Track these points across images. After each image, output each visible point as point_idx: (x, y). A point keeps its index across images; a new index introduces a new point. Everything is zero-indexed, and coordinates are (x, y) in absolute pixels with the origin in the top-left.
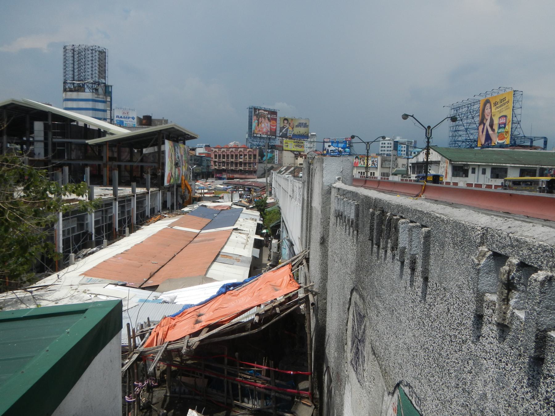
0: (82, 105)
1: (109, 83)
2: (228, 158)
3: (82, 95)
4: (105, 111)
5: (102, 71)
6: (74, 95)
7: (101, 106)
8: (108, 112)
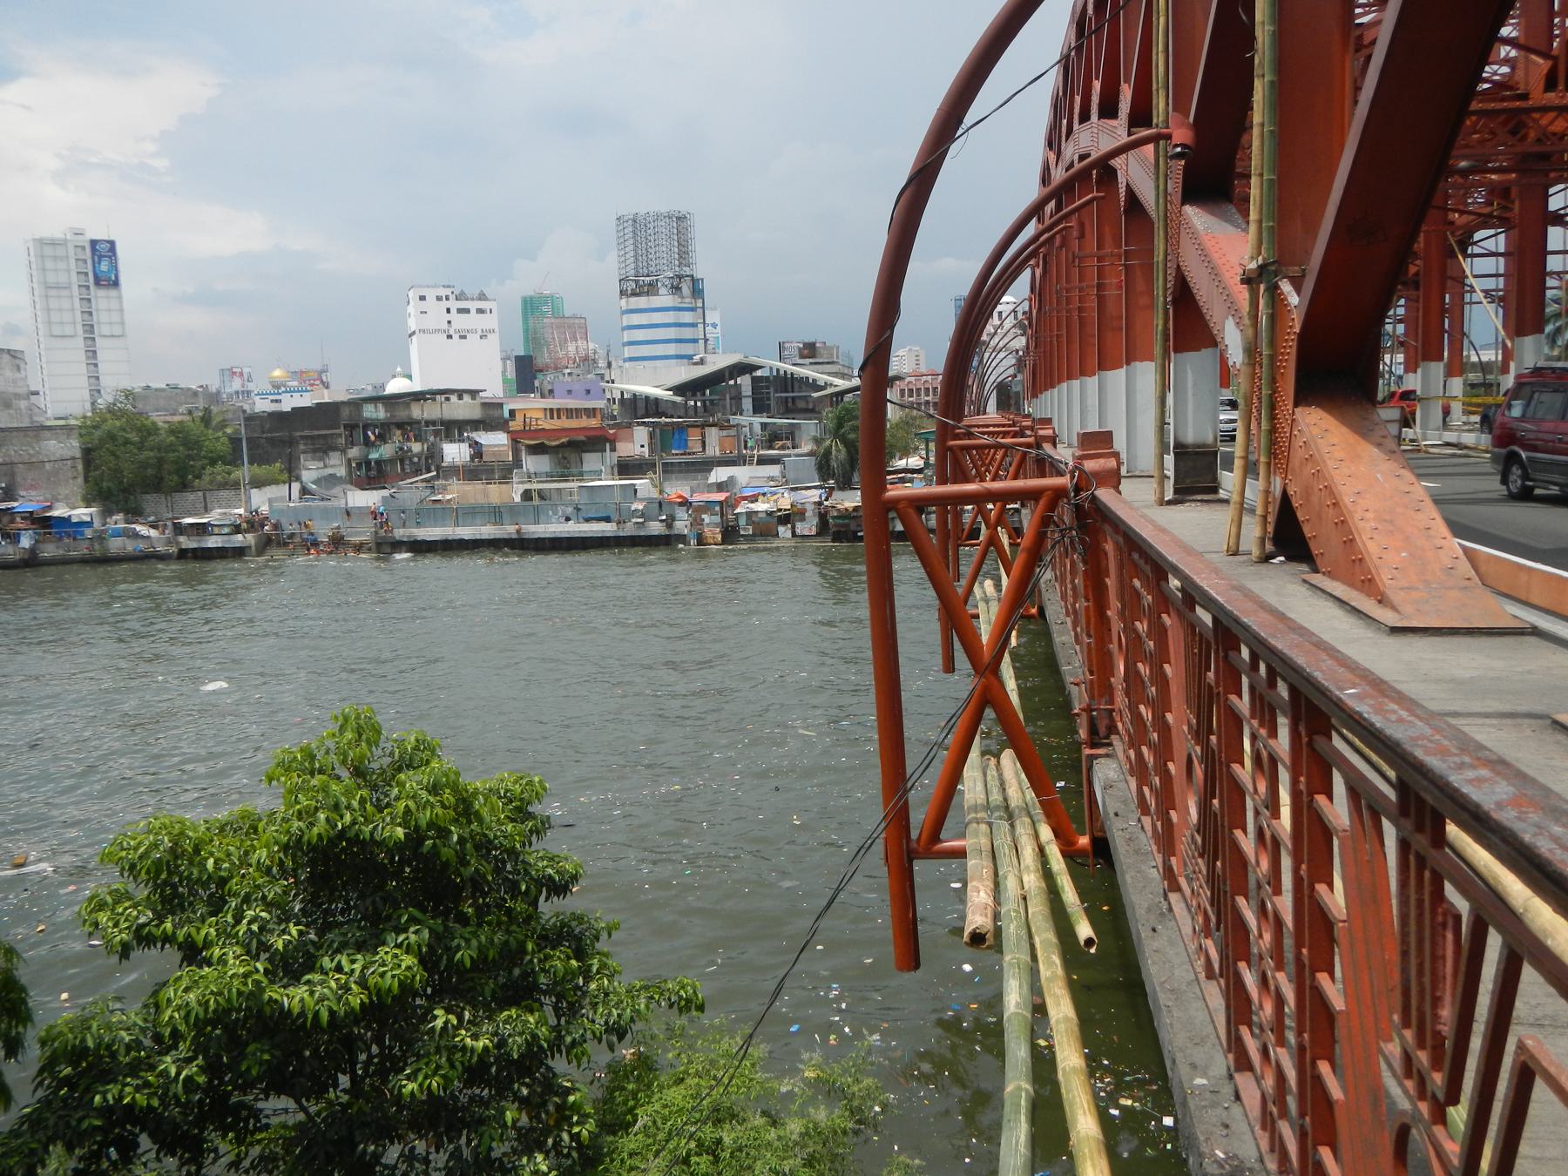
0: (657, 318)
1: (698, 275)
3: (656, 301)
4: (694, 325)
5: (684, 255)
6: (642, 302)
7: (687, 317)
8: (701, 326)
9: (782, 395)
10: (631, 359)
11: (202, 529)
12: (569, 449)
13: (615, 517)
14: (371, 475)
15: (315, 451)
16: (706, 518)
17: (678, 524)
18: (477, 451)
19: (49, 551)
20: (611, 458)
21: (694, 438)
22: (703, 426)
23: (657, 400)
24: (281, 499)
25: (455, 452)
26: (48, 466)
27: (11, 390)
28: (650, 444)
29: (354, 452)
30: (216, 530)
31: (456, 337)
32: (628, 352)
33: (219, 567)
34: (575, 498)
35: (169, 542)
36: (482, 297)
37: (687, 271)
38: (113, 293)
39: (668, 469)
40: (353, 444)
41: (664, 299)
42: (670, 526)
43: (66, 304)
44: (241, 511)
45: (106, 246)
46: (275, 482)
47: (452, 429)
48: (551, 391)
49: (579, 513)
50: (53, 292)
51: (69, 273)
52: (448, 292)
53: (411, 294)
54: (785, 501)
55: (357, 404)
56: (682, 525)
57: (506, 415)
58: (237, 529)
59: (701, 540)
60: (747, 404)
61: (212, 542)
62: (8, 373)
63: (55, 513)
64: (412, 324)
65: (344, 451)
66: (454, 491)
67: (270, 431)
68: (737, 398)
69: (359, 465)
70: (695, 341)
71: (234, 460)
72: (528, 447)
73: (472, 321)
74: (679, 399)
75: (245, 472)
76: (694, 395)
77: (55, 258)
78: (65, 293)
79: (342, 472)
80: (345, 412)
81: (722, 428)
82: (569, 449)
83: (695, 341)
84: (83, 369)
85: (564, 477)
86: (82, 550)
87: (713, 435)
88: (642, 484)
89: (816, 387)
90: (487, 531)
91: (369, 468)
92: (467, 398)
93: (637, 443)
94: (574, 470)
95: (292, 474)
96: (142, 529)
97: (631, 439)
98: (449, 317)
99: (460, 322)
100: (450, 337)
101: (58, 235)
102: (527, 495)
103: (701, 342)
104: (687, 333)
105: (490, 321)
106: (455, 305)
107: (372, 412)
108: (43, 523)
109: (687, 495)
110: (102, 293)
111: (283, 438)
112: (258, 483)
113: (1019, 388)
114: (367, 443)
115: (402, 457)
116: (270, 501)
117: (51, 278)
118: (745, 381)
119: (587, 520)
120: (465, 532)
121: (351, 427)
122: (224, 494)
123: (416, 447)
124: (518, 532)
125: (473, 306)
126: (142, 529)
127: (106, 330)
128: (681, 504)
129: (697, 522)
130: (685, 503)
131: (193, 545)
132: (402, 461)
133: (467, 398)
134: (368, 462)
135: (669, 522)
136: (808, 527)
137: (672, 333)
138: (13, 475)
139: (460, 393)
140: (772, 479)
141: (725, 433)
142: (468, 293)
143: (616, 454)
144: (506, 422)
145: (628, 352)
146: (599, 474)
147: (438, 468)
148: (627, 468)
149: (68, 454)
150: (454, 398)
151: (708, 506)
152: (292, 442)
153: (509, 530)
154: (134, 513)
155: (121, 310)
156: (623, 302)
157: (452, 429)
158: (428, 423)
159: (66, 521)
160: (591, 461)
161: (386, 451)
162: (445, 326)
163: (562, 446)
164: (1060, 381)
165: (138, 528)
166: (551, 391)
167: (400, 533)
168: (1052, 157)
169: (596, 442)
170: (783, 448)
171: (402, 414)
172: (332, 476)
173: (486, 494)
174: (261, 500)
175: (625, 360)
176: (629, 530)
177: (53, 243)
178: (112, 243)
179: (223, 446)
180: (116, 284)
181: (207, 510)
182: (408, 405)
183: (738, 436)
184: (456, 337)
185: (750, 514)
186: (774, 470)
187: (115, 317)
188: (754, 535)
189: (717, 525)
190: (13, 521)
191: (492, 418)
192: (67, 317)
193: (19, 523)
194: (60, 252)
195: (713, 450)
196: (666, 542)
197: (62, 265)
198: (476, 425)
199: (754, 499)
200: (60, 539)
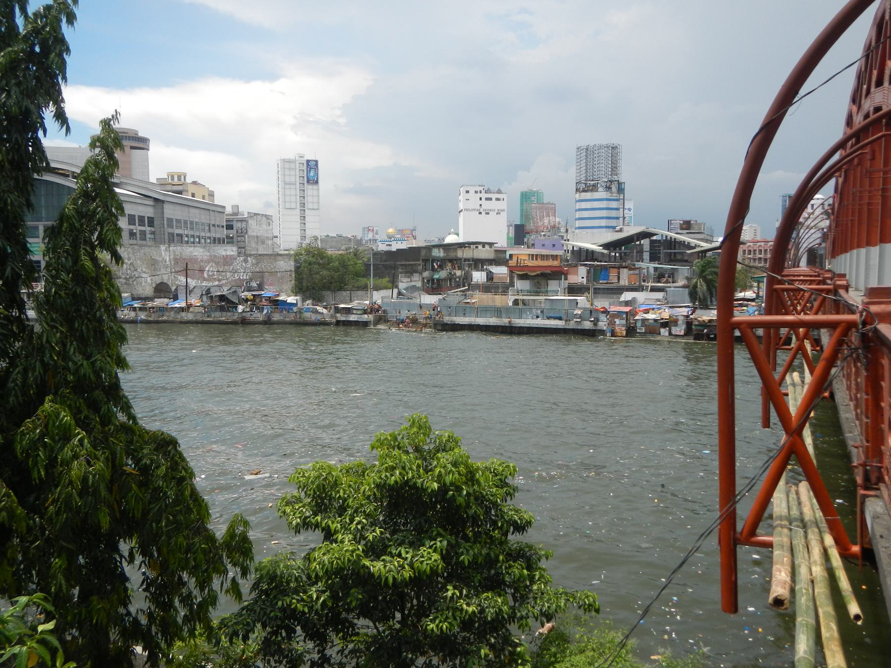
1: (622, 181)
2: (755, 254)
3: (596, 195)
4: (617, 209)
5: (614, 168)
6: (588, 195)
7: (614, 205)
9: (668, 251)
10: (579, 228)
11: (348, 311)
12: (541, 278)
13: (564, 317)
14: (434, 287)
15: (406, 273)
16: (617, 321)
17: (600, 324)
18: (490, 276)
19: (276, 317)
20: (564, 284)
21: (613, 274)
22: (619, 268)
23: (593, 252)
24: (388, 297)
25: (478, 277)
26: (279, 274)
27: (266, 235)
28: (587, 277)
29: (426, 274)
30: (355, 312)
31: (483, 213)
32: (578, 224)
33: (354, 331)
34: (543, 305)
35: (332, 316)
36: (499, 192)
37: (616, 178)
38: (315, 187)
39: (597, 291)
40: (426, 270)
41: (601, 194)
42: (595, 324)
43: (293, 192)
44: (367, 302)
45: (312, 163)
46: (386, 288)
47: (478, 264)
48: (533, 245)
49: (543, 314)
50: (287, 186)
51: (295, 177)
52: (481, 189)
53: (462, 189)
54: (666, 314)
55: (429, 248)
56: (603, 324)
57: (508, 257)
58: (365, 312)
59: (613, 334)
60: (646, 256)
61: (353, 318)
62: (264, 226)
63: (281, 298)
64: (461, 206)
65: (421, 273)
66: (477, 298)
67: (385, 261)
68: (641, 252)
69: (428, 281)
70: (618, 218)
71: (366, 275)
72: (518, 275)
73: (493, 205)
74: (605, 252)
75: (371, 282)
76: (615, 249)
77: (290, 169)
78: (293, 186)
79: (419, 284)
80: (423, 253)
81: (630, 269)
82: (541, 278)
83: (618, 218)
84: (298, 226)
85: (537, 293)
86: (291, 317)
87: (624, 273)
88: (581, 299)
89: (689, 247)
90: (493, 321)
91: (433, 283)
92: (487, 247)
93: (580, 276)
94: (543, 290)
95: (394, 284)
96: (320, 309)
97: (576, 273)
98: (480, 202)
99: (487, 205)
100: (480, 213)
101: (292, 157)
102: (516, 302)
103: (621, 219)
104: (614, 214)
105: (502, 205)
106: (484, 196)
107: (436, 253)
108: (275, 303)
109: (607, 307)
110: (310, 187)
111: (392, 265)
112: (377, 288)
113: (822, 252)
114: (433, 269)
115: (451, 277)
116: (382, 298)
117: (287, 179)
118: (645, 242)
119: (549, 318)
120: (481, 321)
121: (426, 261)
122: (360, 293)
123: (458, 273)
124: (510, 322)
125: (494, 196)
126: (320, 309)
127: (310, 206)
128: (603, 312)
129: (611, 323)
130: (605, 312)
131: (343, 319)
132: (450, 280)
133: (487, 247)
134: (433, 280)
135: (595, 322)
136: (680, 330)
137: (604, 213)
138: (263, 277)
139: (484, 244)
140: (658, 300)
141: (632, 272)
142: (492, 189)
143: (567, 282)
144: (507, 261)
145: (578, 224)
146: (557, 293)
147: (469, 285)
148: (573, 290)
149: (288, 268)
150: (480, 247)
151: (619, 314)
152: (395, 268)
153: (504, 321)
154: (318, 300)
155: (318, 196)
156: (577, 195)
157: (478, 264)
158: (466, 260)
159: (285, 302)
160: (553, 285)
161: (443, 274)
162: (478, 207)
163: (537, 275)
164: (852, 248)
165: (318, 308)
166: (533, 245)
167: (447, 319)
168: (855, 108)
169: (557, 274)
170: (667, 282)
171: (452, 255)
172: (414, 286)
173: (493, 301)
174: (378, 297)
175: (576, 228)
176: (572, 325)
177: (290, 161)
178: (316, 162)
179: (360, 266)
180: (317, 182)
181: (351, 301)
182: (456, 250)
183: (640, 274)
184: (483, 213)
185: (644, 320)
186: (660, 295)
187: (315, 199)
188: (645, 333)
189: (623, 326)
190: (261, 301)
191: (500, 259)
192: (293, 199)
193: (264, 302)
194: (292, 166)
195: (624, 282)
196: (592, 334)
197: (293, 173)
198: (491, 262)
199: (647, 311)
200: (282, 312)
